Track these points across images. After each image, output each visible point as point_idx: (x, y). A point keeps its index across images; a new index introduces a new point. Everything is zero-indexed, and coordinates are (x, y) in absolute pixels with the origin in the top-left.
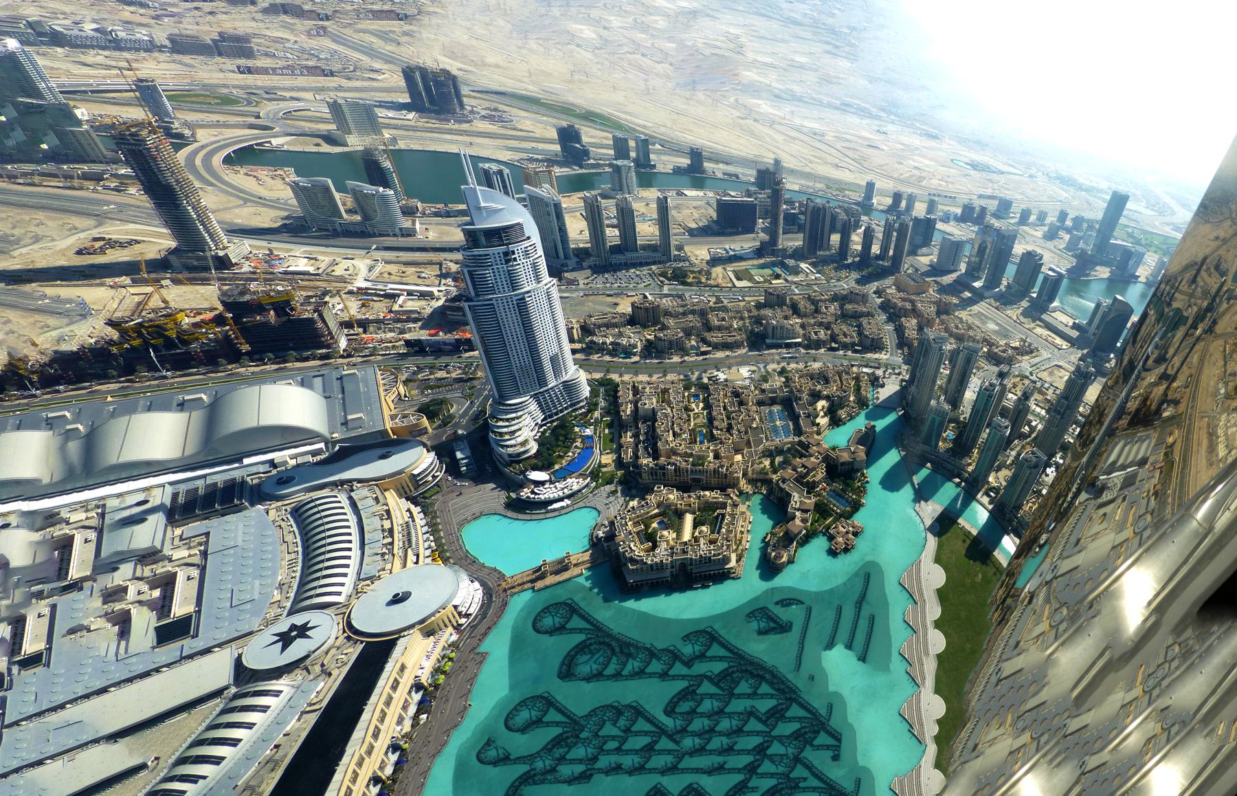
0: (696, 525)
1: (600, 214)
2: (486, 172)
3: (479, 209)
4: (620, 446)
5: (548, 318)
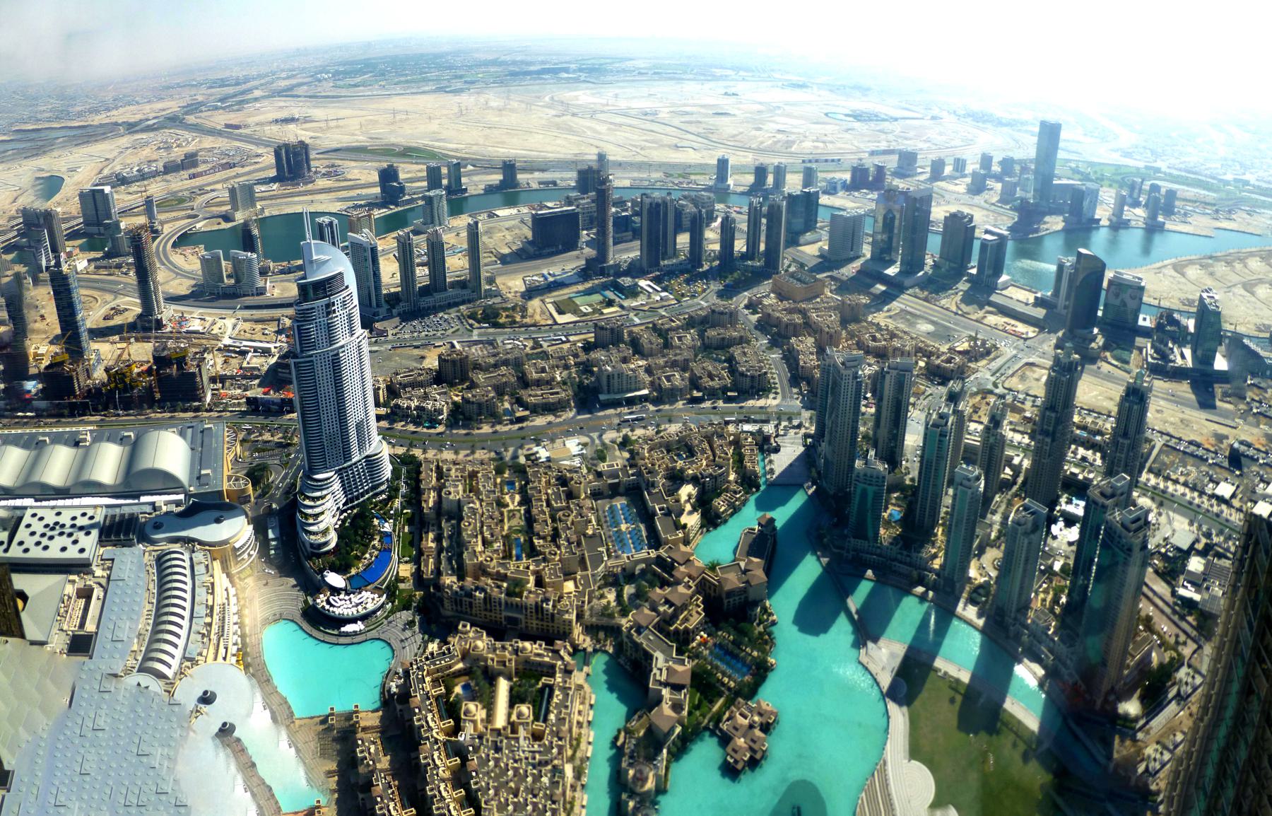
0: (514, 699)
1: (411, 252)
3: (311, 262)
4: (420, 553)
5: (357, 377)
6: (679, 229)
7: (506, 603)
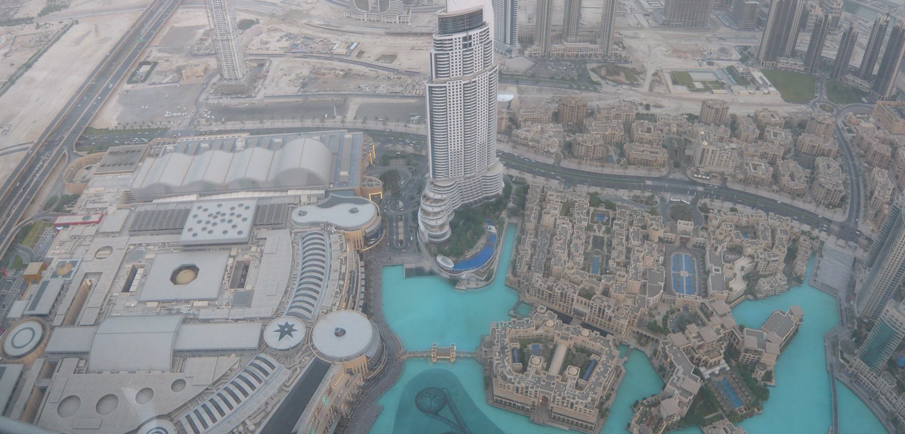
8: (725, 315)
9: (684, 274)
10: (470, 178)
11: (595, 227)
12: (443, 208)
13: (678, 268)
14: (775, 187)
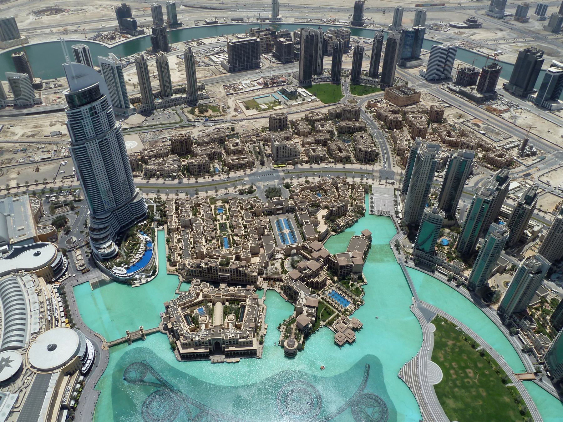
2: (76, 51)
6: (325, 53)
7: (220, 270)
8: (320, 249)
9: (286, 231)
10: (121, 208)
11: (218, 217)
12: (107, 233)
13: (280, 229)
14: (330, 160)
